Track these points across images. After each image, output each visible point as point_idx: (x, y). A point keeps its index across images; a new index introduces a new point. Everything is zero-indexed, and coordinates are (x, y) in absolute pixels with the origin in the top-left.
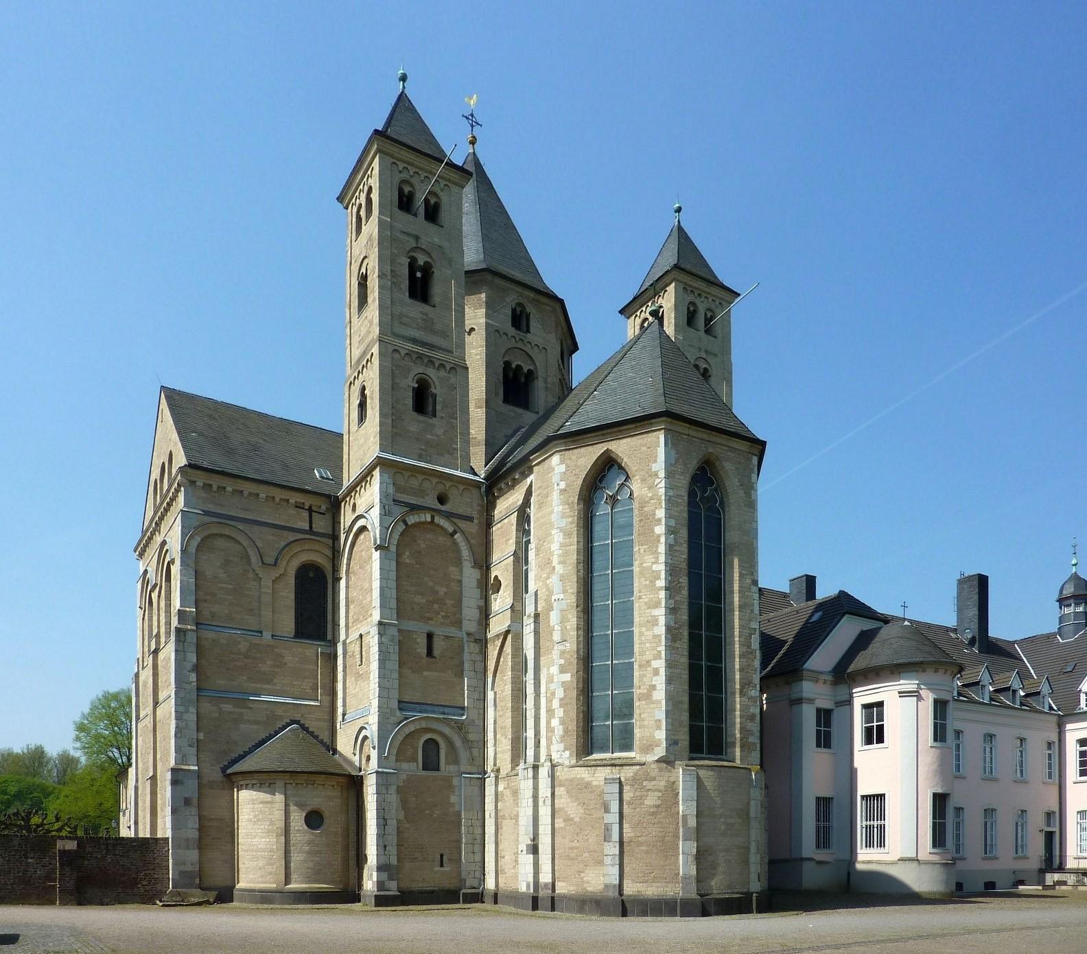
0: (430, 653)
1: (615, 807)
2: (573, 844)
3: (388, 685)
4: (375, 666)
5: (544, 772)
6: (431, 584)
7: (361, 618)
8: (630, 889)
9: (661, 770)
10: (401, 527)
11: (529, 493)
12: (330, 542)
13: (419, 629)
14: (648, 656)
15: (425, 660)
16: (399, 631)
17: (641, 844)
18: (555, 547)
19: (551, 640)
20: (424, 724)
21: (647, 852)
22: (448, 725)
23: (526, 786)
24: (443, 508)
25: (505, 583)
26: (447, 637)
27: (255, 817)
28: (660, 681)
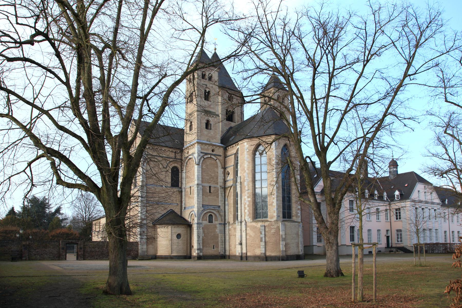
0: (210, 192)
1: (263, 233)
2: (252, 242)
3: (200, 201)
4: (196, 196)
5: (243, 224)
8: (268, 254)
9: (275, 223)
10: (203, 159)
11: (238, 150)
13: (207, 185)
15: (209, 194)
16: (202, 186)
17: (270, 242)
18: (246, 166)
19: (245, 189)
20: (209, 211)
21: (272, 244)
23: (238, 227)
24: (213, 153)
26: (215, 187)
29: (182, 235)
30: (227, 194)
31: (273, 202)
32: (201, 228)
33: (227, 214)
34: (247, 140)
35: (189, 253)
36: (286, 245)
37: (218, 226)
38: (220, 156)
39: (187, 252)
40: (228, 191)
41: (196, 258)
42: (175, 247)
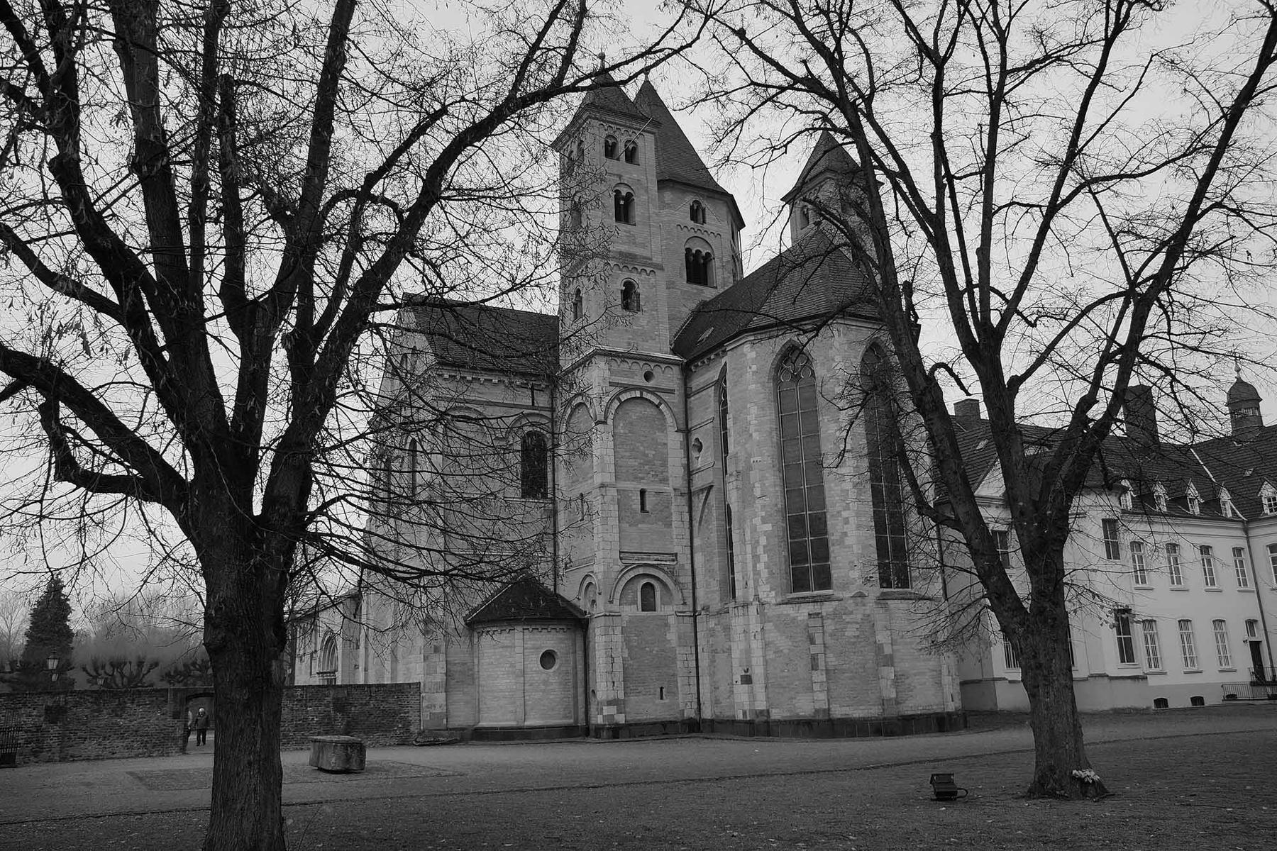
0: (643, 508)
2: (785, 674)
5: (753, 610)
6: (642, 448)
7: (581, 479)
8: (838, 712)
10: (616, 404)
12: (548, 414)
13: (633, 487)
15: (639, 515)
19: (752, 495)
20: (641, 571)
22: (663, 570)
24: (651, 384)
25: (707, 445)
28: (851, 528)
30: (697, 515)
31: (845, 534)
32: (618, 630)
34: (752, 338)
35: (581, 716)
37: (672, 620)
38: (672, 392)
40: (701, 505)
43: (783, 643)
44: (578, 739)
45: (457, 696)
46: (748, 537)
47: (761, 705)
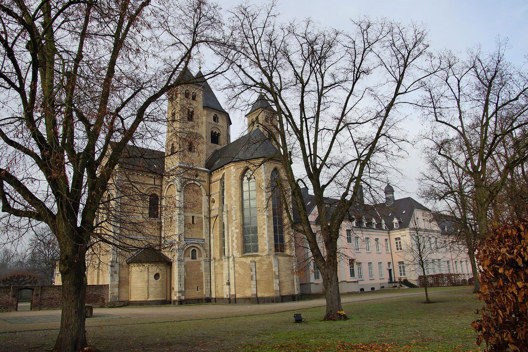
0: (193, 223)
1: (254, 270)
5: (231, 259)
8: (259, 295)
9: (267, 258)
11: (224, 175)
13: (190, 215)
14: (262, 224)
17: (262, 281)
19: (232, 219)
21: (264, 283)
22: (199, 245)
27: (138, 276)
28: (266, 232)
29: (160, 275)
30: (212, 225)
31: (264, 233)
33: (212, 248)
34: (234, 164)
35: (168, 297)
36: (280, 284)
37: (203, 263)
38: (205, 182)
39: (167, 296)
41: (177, 303)
42: (151, 290)
43: (241, 271)
44: (167, 305)
45: (123, 290)
46: (230, 234)
47: (233, 293)
